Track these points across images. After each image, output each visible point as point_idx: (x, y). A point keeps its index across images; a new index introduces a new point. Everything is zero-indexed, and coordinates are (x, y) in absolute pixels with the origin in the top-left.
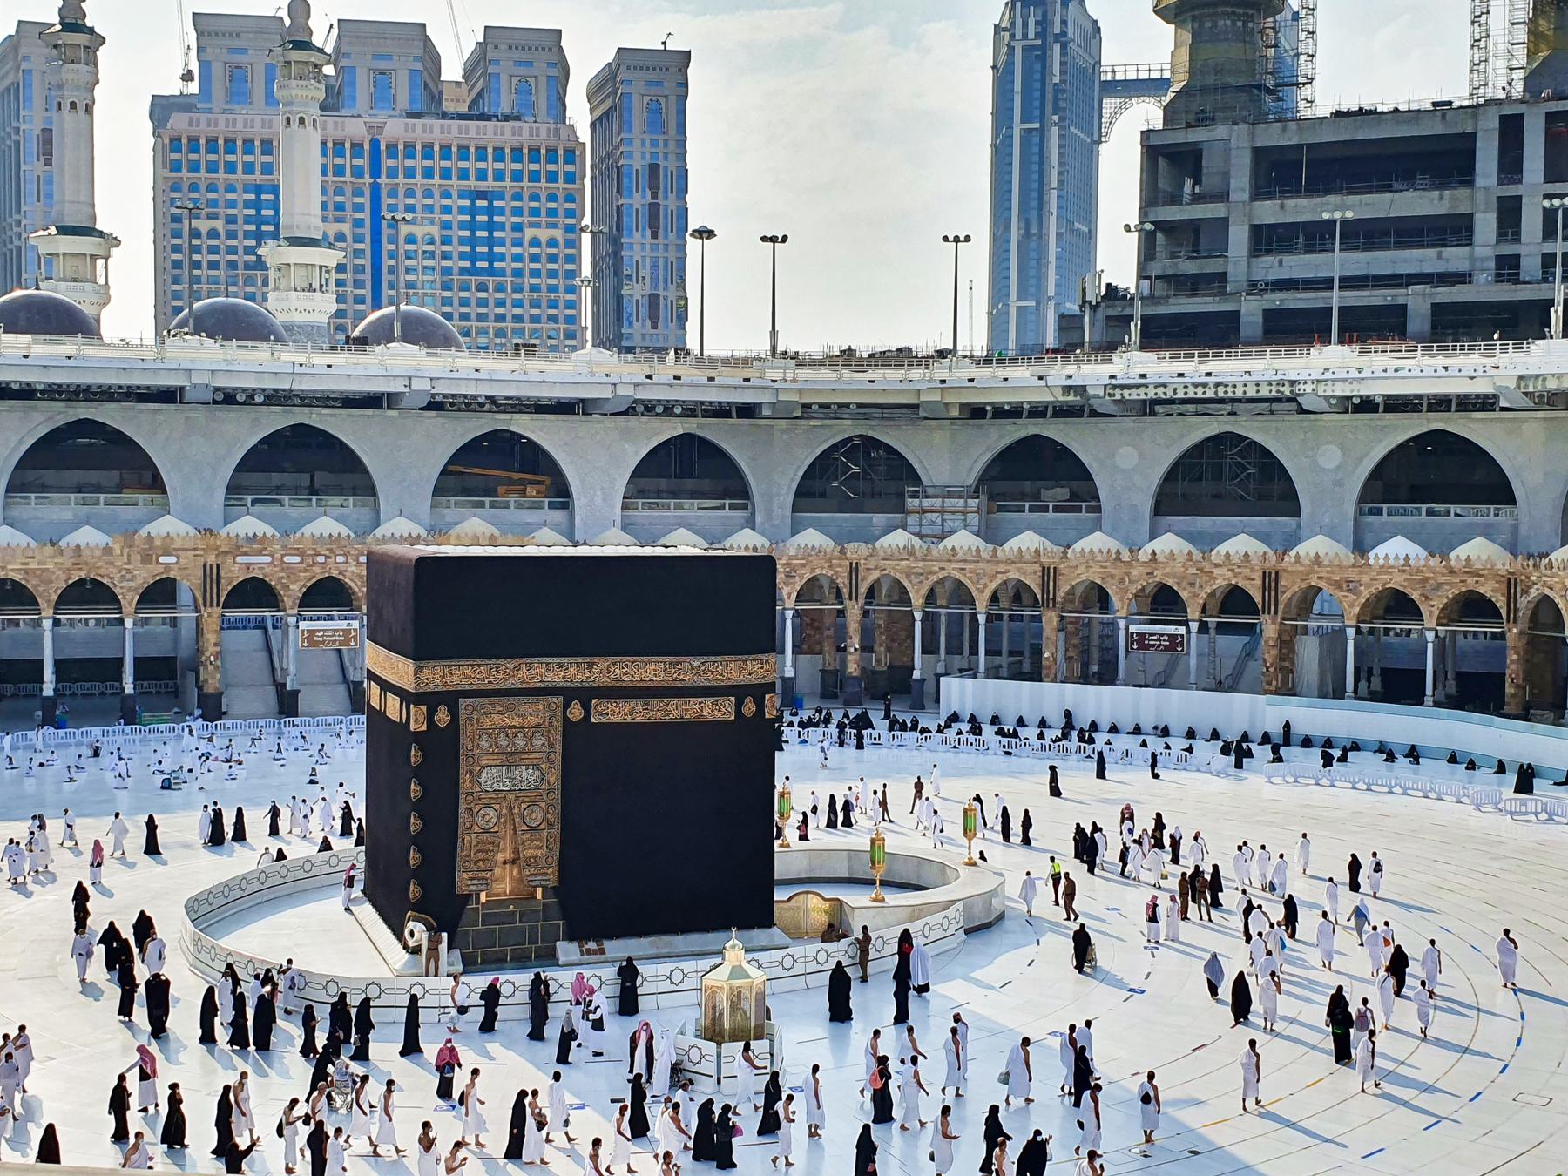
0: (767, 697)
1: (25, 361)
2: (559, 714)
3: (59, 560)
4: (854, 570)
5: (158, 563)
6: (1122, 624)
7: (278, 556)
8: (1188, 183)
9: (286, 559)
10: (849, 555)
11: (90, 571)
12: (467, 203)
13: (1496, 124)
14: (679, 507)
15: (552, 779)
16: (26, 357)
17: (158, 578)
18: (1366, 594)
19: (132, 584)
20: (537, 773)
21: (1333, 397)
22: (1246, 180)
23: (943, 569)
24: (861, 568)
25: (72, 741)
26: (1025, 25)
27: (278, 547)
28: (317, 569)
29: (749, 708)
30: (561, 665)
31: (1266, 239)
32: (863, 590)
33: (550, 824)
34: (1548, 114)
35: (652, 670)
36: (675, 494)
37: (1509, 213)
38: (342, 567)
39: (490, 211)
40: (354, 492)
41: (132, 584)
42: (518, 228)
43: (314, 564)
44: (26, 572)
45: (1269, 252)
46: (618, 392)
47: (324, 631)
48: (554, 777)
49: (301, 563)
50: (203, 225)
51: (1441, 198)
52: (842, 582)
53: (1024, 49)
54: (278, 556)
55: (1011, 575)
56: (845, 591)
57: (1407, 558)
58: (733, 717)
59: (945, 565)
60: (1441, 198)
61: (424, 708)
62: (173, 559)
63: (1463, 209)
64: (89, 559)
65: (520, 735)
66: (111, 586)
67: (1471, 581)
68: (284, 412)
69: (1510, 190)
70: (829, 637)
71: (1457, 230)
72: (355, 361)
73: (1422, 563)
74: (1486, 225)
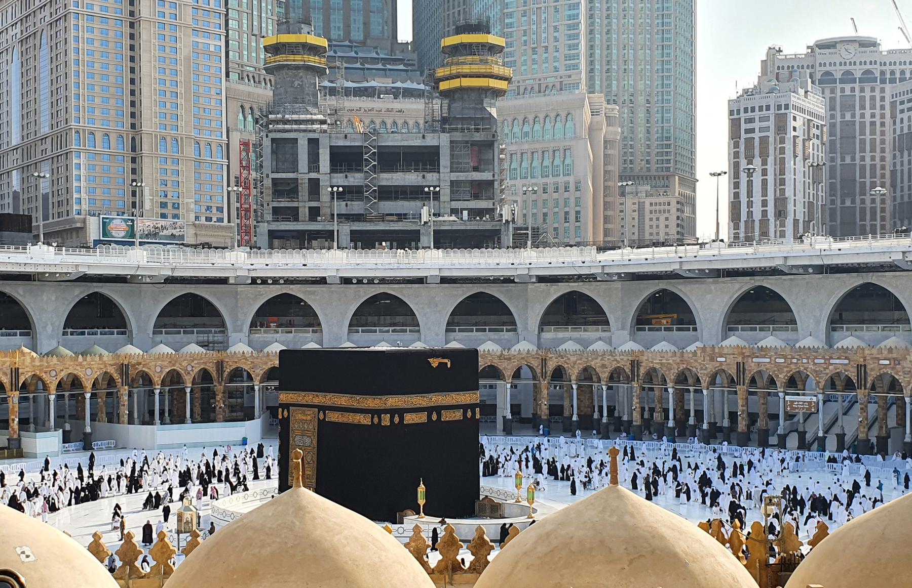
1: (550, 265)
7: (773, 358)
9: (778, 360)
11: (687, 364)
14: (585, 331)
16: (695, 257)
19: (705, 372)
25: (687, 450)
27: (773, 353)
28: (793, 367)
29: (376, 420)
30: (317, 396)
35: (343, 400)
36: (863, 322)
38: (806, 365)
40: (898, 321)
41: (705, 372)
43: (792, 363)
44: (661, 364)
47: (798, 402)
48: (315, 442)
49: (785, 362)
54: (773, 358)
62: (723, 359)
64: (687, 358)
68: (894, 276)
72: (855, 245)
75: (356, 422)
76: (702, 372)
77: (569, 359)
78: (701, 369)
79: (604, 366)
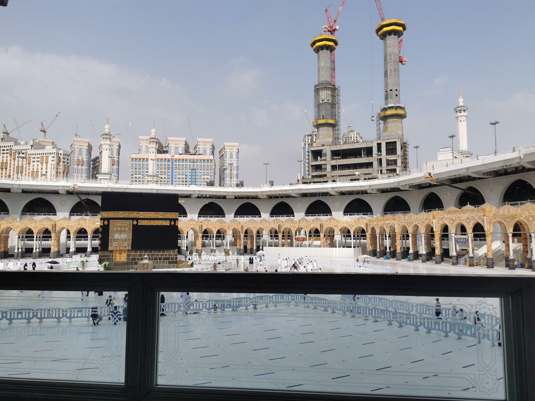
0: (176, 221)
2: (132, 223)
3: (75, 223)
4: (242, 227)
5: (96, 224)
6: (294, 236)
8: (319, 158)
10: (241, 224)
12: (191, 171)
13: (376, 145)
15: (130, 237)
17: (96, 227)
18: (340, 228)
19: (90, 229)
20: (127, 235)
21: (335, 191)
22: (330, 156)
23: (259, 226)
24: (244, 226)
26: (308, 140)
29: (173, 223)
30: (132, 213)
31: (334, 167)
32: (244, 231)
33: (129, 246)
34: (386, 143)
37: (380, 161)
39: (195, 173)
42: (201, 176)
45: (335, 170)
46: (195, 192)
48: (131, 237)
50: (137, 176)
51: (367, 159)
52: (240, 229)
53: (308, 144)
55: (272, 227)
56: (240, 231)
57: (347, 220)
58: (169, 225)
59: (259, 225)
60: (367, 159)
61: (103, 221)
63: (371, 161)
65: (123, 228)
66: (86, 229)
67: (359, 224)
69: (380, 157)
70: (238, 242)
71: (369, 165)
73: (350, 221)
74: (375, 164)
75: (160, 224)
76: (88, 228)
77: (15, 224)
78: (88, 227)
79: (35, 227)
